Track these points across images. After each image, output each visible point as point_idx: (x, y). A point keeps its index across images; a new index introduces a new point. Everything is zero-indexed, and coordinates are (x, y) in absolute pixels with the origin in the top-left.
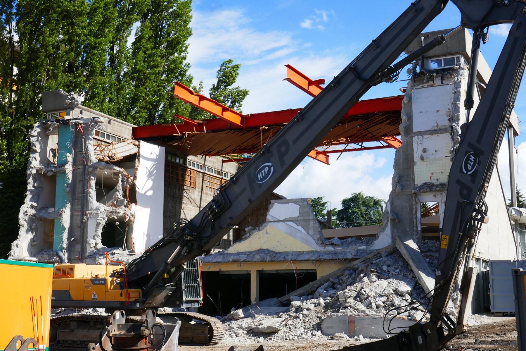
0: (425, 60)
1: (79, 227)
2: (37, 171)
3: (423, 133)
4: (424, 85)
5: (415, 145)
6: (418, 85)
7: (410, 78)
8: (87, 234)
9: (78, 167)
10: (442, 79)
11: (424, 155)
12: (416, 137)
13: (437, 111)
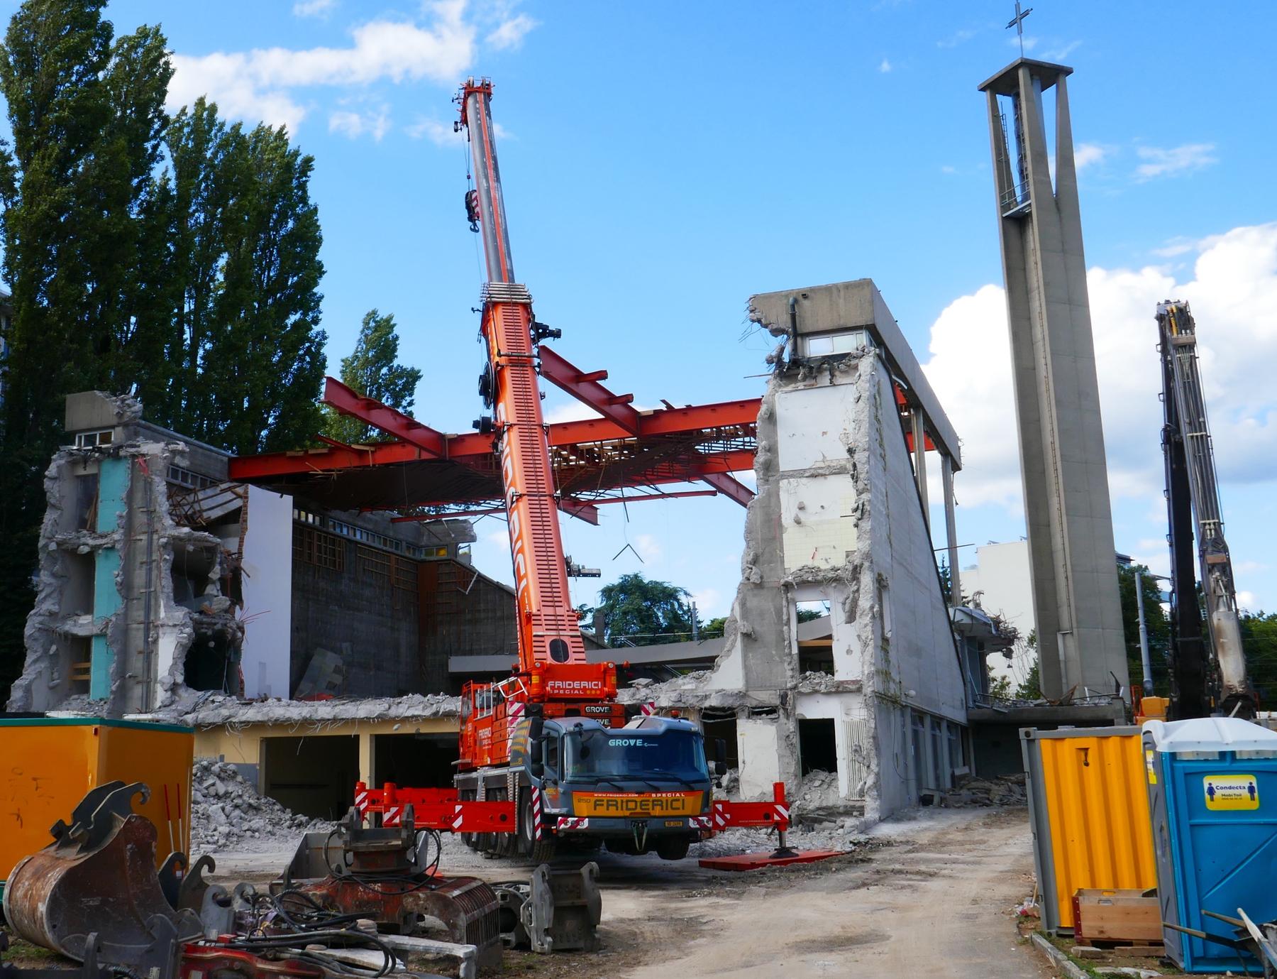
0: (799, 340)
1: (140, 652)
2: (58, 544)
3: (798, 474)
4: (799, 384)
5: (783, 497)
6: (787, 385)
7: (771, 372)
8: (156, 665)
9: (138, 538)
10: (832, 375)
11: (802, 516)
12: (785, 481)
13: (824, 433)
